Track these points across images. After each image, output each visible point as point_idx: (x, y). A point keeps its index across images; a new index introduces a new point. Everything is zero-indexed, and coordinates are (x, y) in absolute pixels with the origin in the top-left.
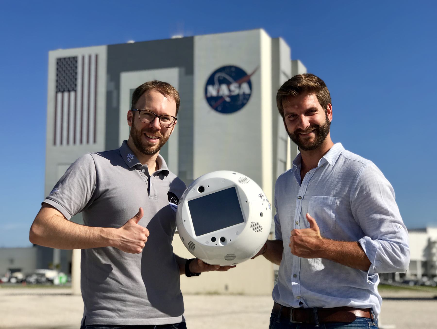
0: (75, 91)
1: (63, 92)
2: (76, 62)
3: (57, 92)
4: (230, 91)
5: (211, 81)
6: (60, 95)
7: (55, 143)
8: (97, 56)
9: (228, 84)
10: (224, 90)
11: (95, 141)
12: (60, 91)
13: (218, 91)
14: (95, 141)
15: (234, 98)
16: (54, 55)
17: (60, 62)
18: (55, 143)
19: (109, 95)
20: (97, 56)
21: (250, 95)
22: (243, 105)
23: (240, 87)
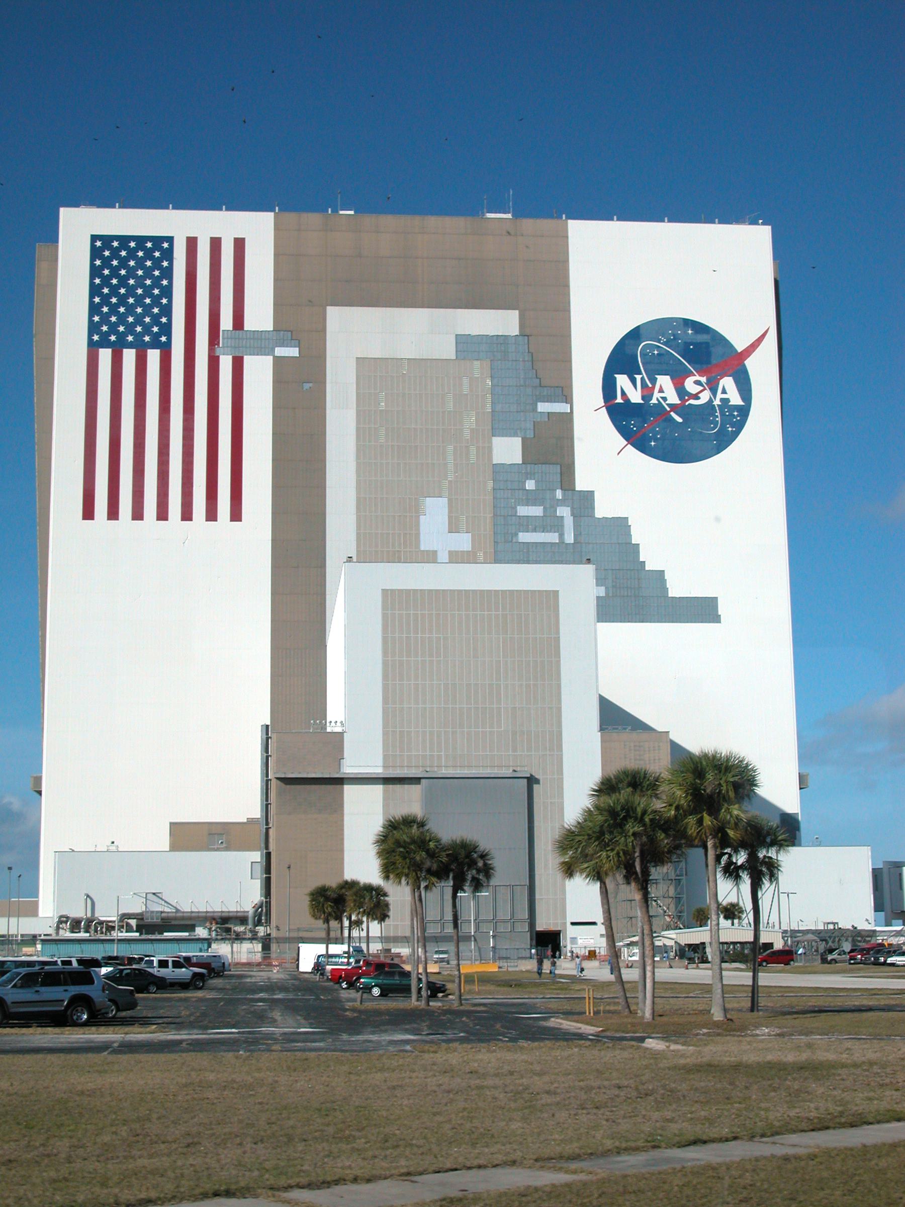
2: (168, 254)
3: (93, 348)
4: (681, 392)
5: (622, 360)
6: (105, 356)
7: (88, 513)
8: (239, 244)
10: (666, 389)
12: (104, 342)
13: (647, 393)
14: (236, 515)
16: (79, 227)
17: (102, 246)
18: (88, 513)
20: (239, 244)
21: (744, 411)
22: (723, 440)
23: (713, 386)
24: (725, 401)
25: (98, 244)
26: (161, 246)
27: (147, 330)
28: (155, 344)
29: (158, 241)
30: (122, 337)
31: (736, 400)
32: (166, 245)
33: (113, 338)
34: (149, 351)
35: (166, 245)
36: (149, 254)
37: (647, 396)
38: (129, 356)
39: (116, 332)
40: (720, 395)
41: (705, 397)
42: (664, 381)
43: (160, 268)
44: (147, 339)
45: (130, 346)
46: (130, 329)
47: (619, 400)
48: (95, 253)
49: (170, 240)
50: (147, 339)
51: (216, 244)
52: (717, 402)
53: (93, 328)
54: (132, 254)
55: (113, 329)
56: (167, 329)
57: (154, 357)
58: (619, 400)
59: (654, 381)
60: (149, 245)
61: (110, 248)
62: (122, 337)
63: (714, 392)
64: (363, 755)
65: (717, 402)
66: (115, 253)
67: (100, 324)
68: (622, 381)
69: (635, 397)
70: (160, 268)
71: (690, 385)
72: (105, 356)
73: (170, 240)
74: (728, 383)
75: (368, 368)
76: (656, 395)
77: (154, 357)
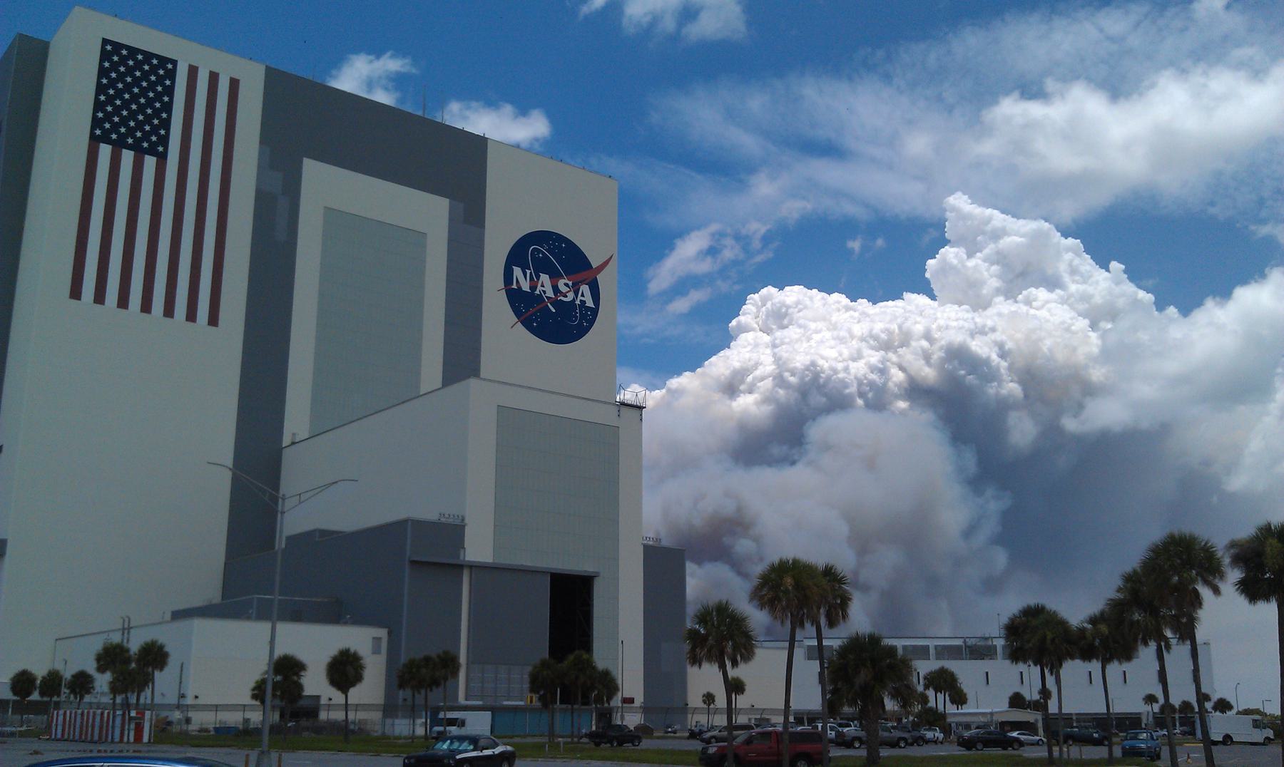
0: (162, 158)
1: (119, 145)
2: (172, 75)
3: (95, 141)
4: (556, 289)
5: (517, 255)
6: (105, 151)
7: (76, 293)
8: (234, 84)
9: (555, 276)
11: (213, 320)
14: (213, 320)
15: (566, 309)
17: (112, 52)
18: (76, 293)
19: (264, 202)
20: (234, 84)
21: (595, 312)
24: (583, 302)
25: (109, 48)
26: (166, 67)
27: (146, 136)
28: (152, 151)
29: (163, 61)
30: (122, 138)
31: (590, 303)
32: (170, 66)
33: (114, 136)
34: (147, 157)
35: (170, 66)
36: (154, 69)
37: (533, 288)
38: (128, 157)
39: (118, 133)
40: (580, 297)
41: (570, 296)
42: (545, 278)
43: (163, 85)
44: (145, 145)
45: (129, 147)
46: (131, 132)
47: (514, 286)
48: (105, 55)
49: (174, 63)
50: (145, 145)
51: (214, 78)
52: (578, 302)
53: (96, 123)
54: (139, 65)
55: (115, 127)
56: (164, 141)
57: (150, 162)
58: (514, 286)
59: (538, 277)
60: (155, 62)
61: (119, 55)
62: (122, 138)
63: (576, 293)
64: (479, 547)
65: (578, 302)
66: (123, 60)
67: (103, 121)
68: (517, 271)
69: (526, 287)
70: (163, 85)
71: (561, 284)
72: (105, 151)
73: (174, 63)
74: (585, 289)
75: (335, 219)
76: (539, 288)
77: (150, 162)
